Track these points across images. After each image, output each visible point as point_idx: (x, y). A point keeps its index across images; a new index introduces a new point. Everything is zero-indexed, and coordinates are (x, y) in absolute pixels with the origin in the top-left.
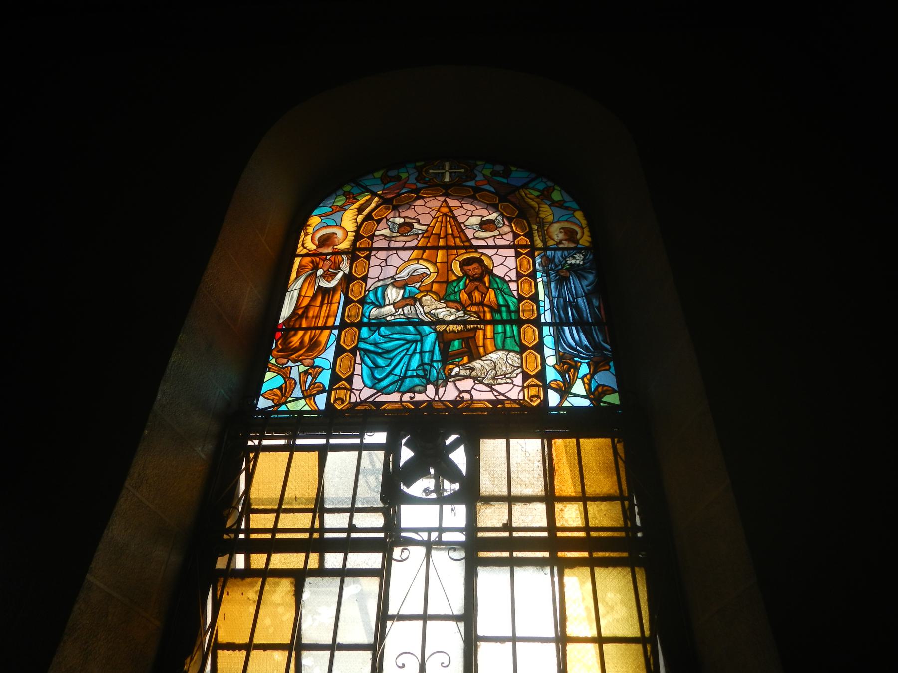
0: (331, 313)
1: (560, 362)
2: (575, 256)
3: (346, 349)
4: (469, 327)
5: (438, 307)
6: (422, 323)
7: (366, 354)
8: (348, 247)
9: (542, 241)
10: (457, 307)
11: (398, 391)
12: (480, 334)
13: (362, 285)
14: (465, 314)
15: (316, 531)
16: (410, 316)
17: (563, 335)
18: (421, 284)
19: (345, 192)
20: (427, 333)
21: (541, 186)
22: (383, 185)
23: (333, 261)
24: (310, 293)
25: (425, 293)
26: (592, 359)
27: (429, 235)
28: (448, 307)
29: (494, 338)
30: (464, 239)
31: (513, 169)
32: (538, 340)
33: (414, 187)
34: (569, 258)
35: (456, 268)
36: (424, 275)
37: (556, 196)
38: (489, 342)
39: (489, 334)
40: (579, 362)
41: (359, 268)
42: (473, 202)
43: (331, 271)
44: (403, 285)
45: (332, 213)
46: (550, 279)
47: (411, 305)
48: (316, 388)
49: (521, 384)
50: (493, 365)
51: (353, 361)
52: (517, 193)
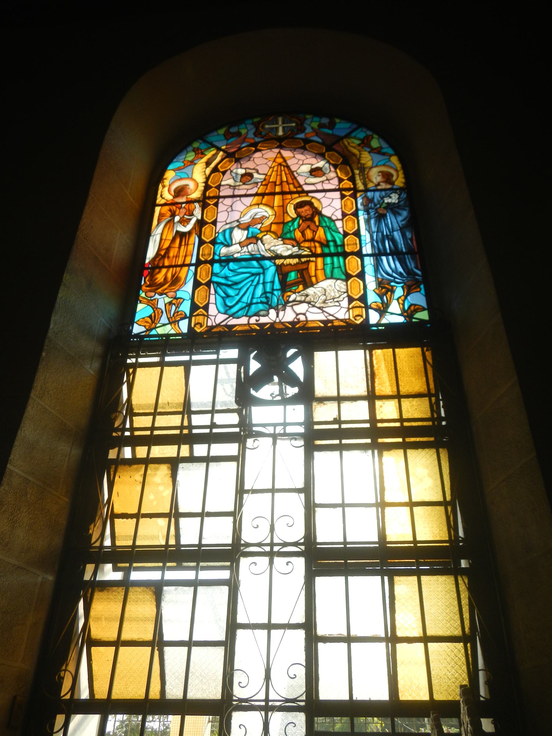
0: (188, 253)
1: (379, 286)
4: (303, 260)
5: (277, 244)
6: (264, 258)
7: (218, 286)
10: (293, 244)
11: (246, 316)
12: (312, 266)
13: (213, 228)
14: (299, 249)
15: (185, 428)
21: (362, 135)
22: (226, 141)
23: (187, 208)
24: (170, 237)
28: (285, 244)
29: (324, 269)
30: (297, 185)
31: (337, 121)
33: (252, 141)
34: (386, 197)
35: (290, 211)
36: (263, 218)
37: (375, 143)
39: (320, 266)
40: (395, 286)
41: (209, 214)
43: (186, 218)
44: (246, 227)
45: (185, 166)
46: (370, 216)
47: (255, 244)
49: (347, 306)
52: (341, 142)
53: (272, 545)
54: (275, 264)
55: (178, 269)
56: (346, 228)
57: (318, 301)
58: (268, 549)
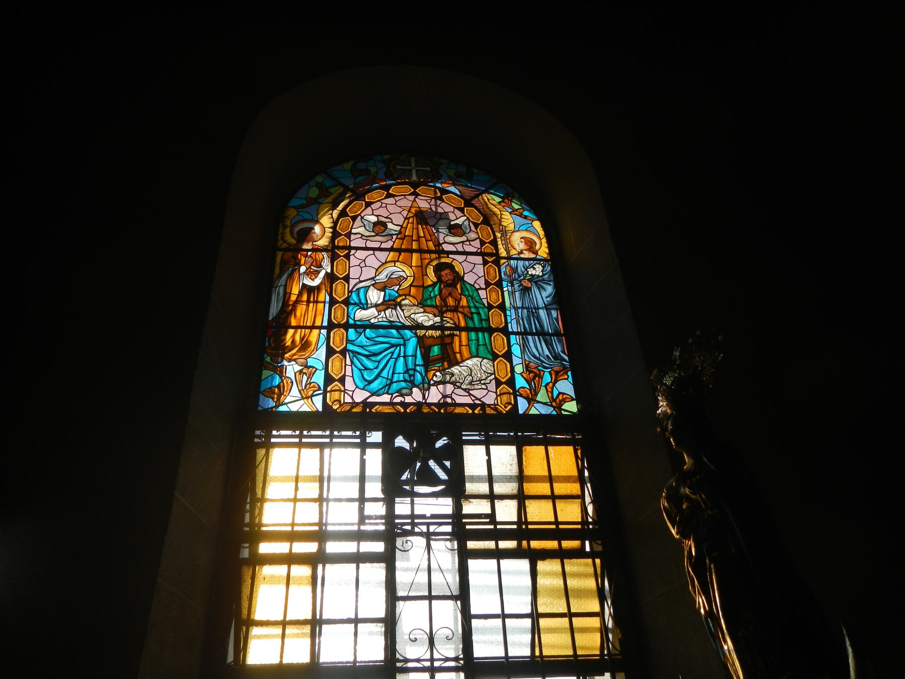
4: (447, 333)
5: (417, 312)
6: (404, 327)
7: (355, 356)
8: (327, 244)
9: (506, 250)
10: (434, 313)
11: (387, 393)
12: (456, 339)
13: (345, 285)
16: (392, 320)
17: (528, 344)
18: (399, 287)
19: (317, 183)
20: (409, 337)
22: (353, 179)
25: (404, 297)
31: (475, 171)
32: (506, 349)
34: (530, 268)
38: (464, 348)
39: (464, 342)
40: (543, 371)
41: (340, 267)
43: (313, 269)
44: (383, 288)
46: (514, 289)
48: (312, 388)
51: (344, 362)
52: (480, 197)
54: (416, 334)
55: (307, 331)
57: (464, 382)
58: (427, 664)
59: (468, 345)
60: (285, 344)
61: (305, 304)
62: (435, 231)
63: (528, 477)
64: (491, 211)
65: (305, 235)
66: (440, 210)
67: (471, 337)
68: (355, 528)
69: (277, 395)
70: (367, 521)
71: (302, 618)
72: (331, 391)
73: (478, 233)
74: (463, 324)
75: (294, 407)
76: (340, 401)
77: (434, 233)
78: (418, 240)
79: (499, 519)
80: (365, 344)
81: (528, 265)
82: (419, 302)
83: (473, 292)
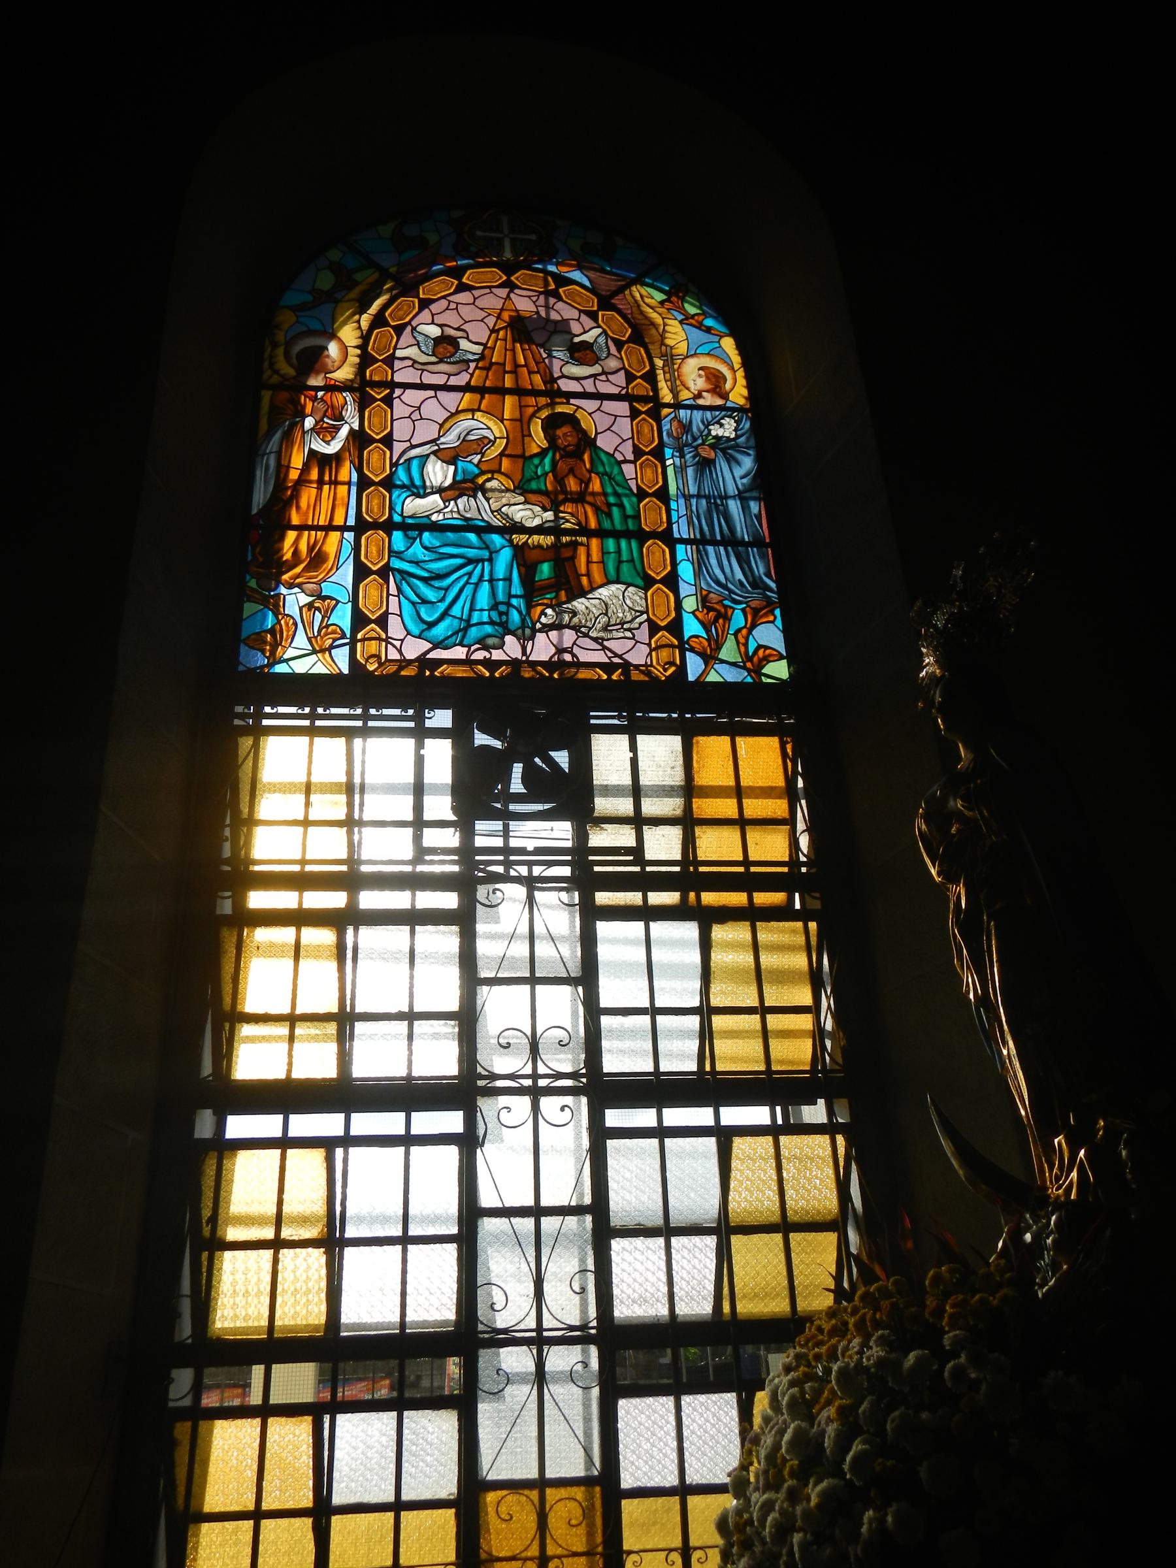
1: (704, 606)
2: (722, 421)
3: (370, 568)
4: (564, 539)
6: (490, 529)
7: (404, 579)
8: (351, 376)
9: (671, 391)
11: (461, 644)
12: (582, 551)
13: (384, 453)
16: (468, 515)
18: (482, 457)
20: (498, 548)
25: (490, 476)
26: (750, 603)
27: (487, 365)
28: (529, 503)
29: (602, 562)
32: (669, 568)
34: (713, 425)
35: (536, 432)
38: (595, 568)
39: (595, 557)
40: (731, 607)
41: (375, 420)
42: (555, 303)
43: (327, 423)
44: (451, 457)
46: (685, 462)
47: (469, 496)
50: (604, 606)
51: (385, 590)
52: (627, 292)
53: (535, 1076)
54: (510, 541)
55: (320, 534)
56: (642, 480)
58: (528, 1082)
59: (602, 562)
60: (282, 556)
61: (315, 486)
62: (545, 355)
63: (701, 787)
64: (647, 318)
65: (313, 359)
66: (554, 316)
67: (608, 548)
68: (408, 869)
69: (271, 645)
70: (427, 858)
71: (322, 1010)
72: (363, 640)
73: (621, 359)
74: (593, 524)
75: (300, 667)
76: (378, 657)
77: (544, 359)
78: (515, 371)
79: (649, 856)
80: (421, 557)
81: (710, 419)
82: (516, 484)
83: (612, 467)
